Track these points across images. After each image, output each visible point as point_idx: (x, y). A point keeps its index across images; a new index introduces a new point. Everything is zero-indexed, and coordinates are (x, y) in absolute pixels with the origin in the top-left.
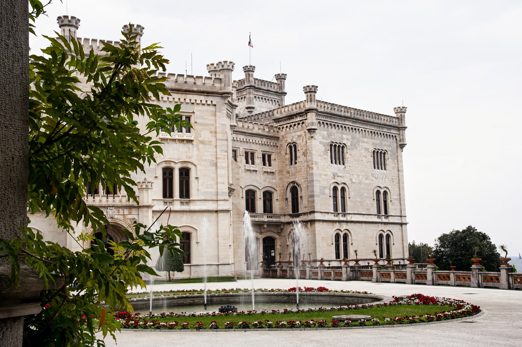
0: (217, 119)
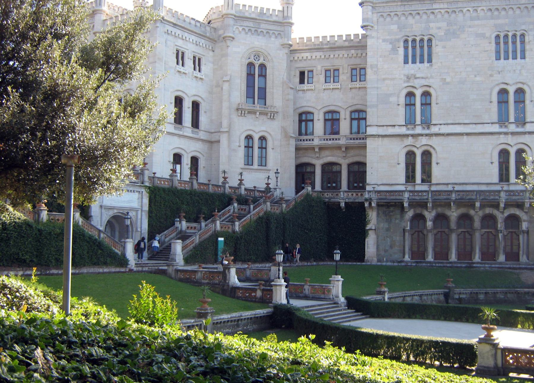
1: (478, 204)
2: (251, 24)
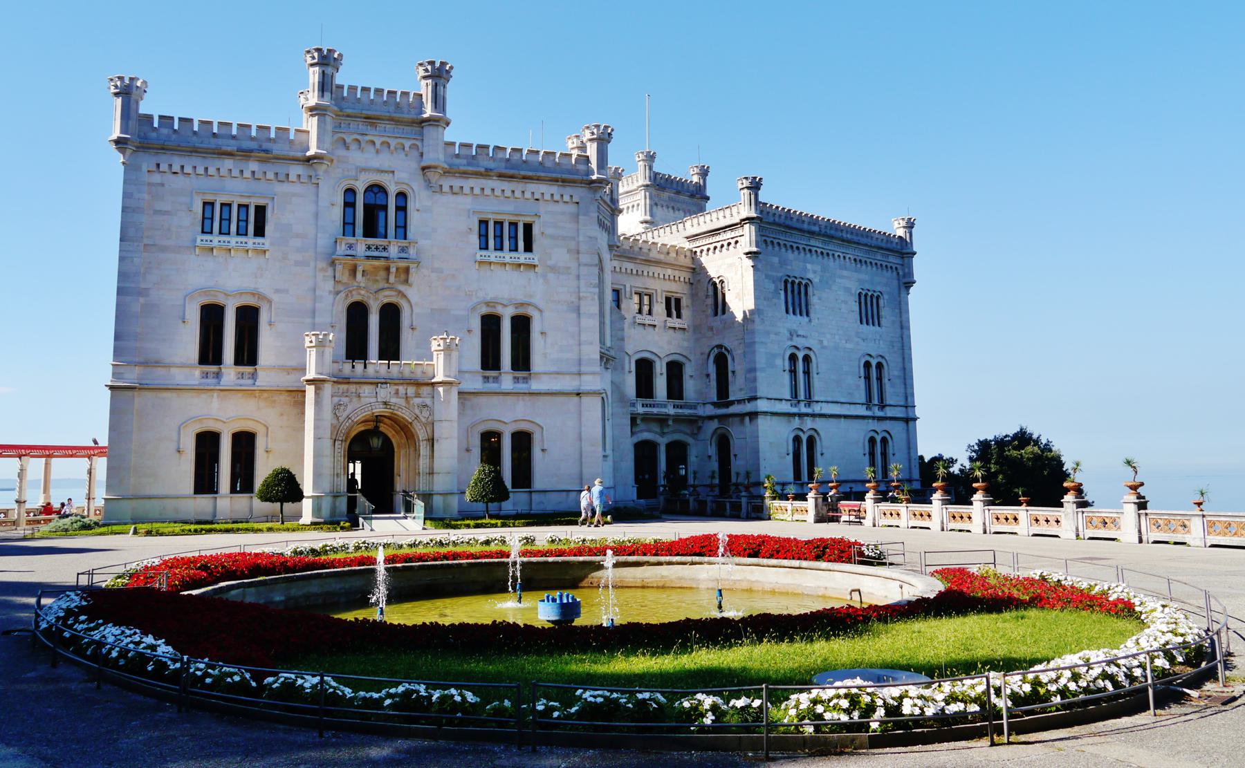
0: (580, 227)
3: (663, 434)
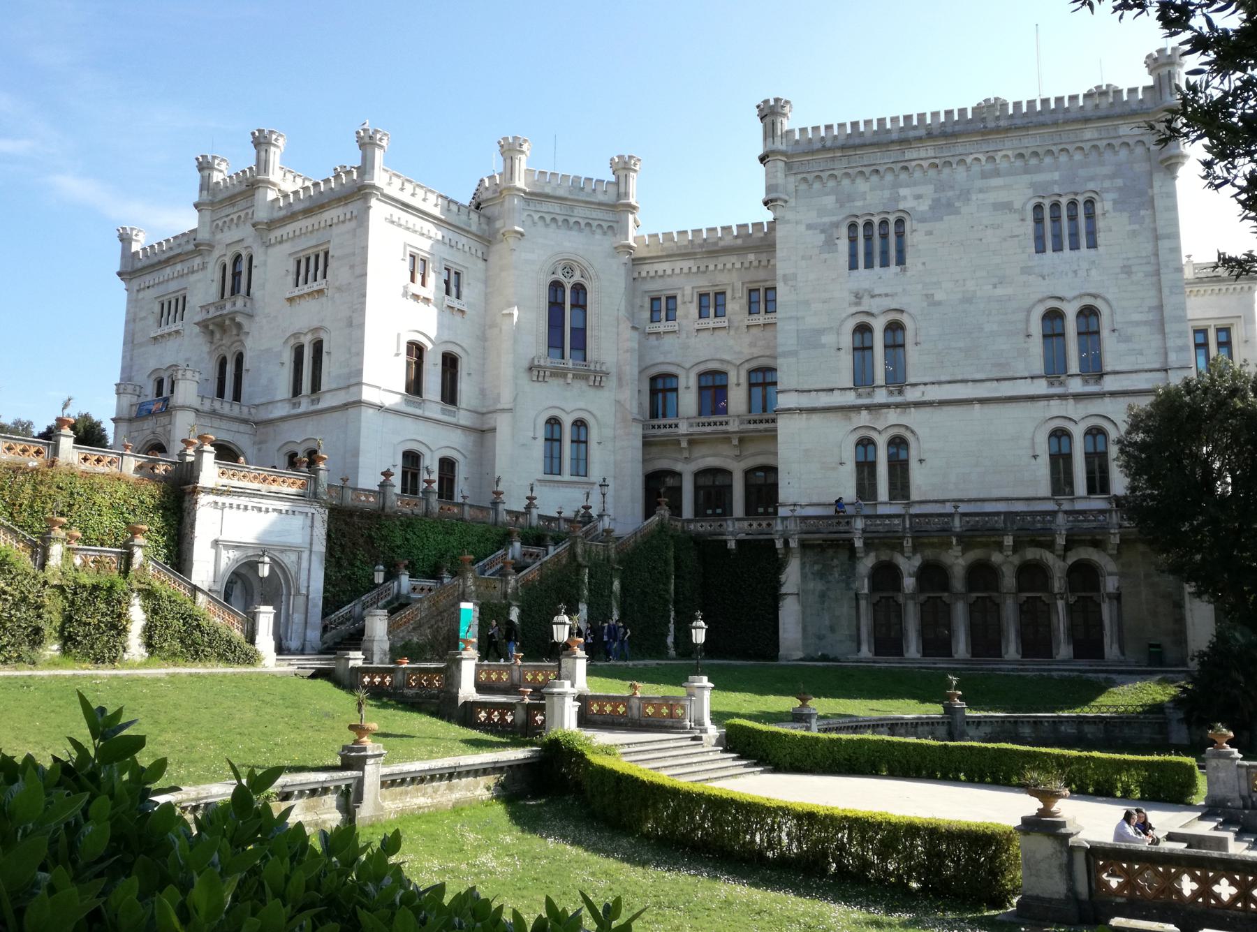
1: (1009, 541)
2: (555, 208)
3: (738, 458)
